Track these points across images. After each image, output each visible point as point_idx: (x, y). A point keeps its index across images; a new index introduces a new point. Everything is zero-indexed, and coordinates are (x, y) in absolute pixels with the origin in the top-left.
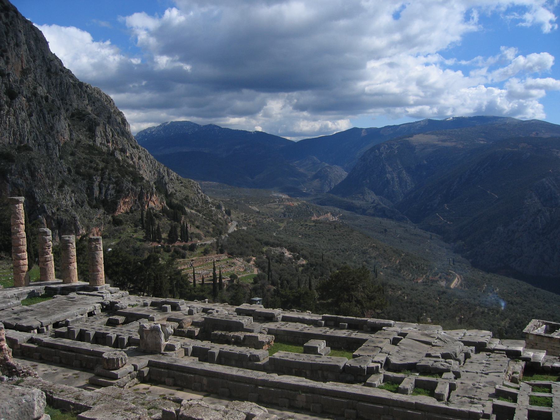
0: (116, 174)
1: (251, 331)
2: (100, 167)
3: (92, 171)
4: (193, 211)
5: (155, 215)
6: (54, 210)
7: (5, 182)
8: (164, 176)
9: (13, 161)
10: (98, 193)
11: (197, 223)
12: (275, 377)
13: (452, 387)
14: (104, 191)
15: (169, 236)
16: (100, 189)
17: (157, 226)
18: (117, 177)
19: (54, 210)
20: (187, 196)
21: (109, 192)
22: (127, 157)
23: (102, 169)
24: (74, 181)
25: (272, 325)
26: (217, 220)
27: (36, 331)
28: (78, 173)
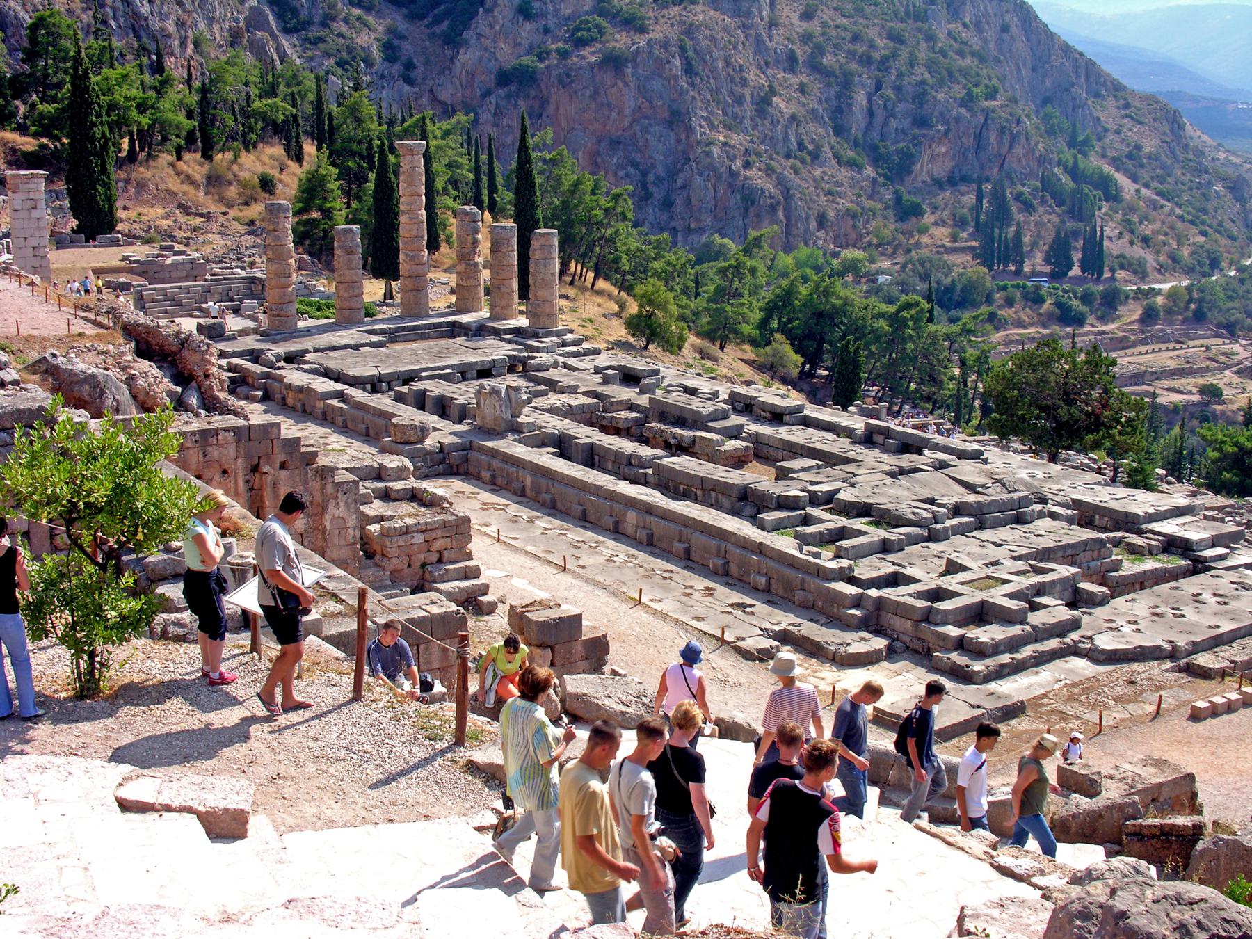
0: (921, 73)
1: (710, 430)
2: (877, 55)
3: (854, 66)
4: (1145, 192)
5: (1018, 197)
6: (737, 165)
7: (620, 84)
8: (1073, 85)
9: (643, 30)
10: (863, 124)
11: (1146, 229)
12: (624, 488)
13: (885, 548)
14: (879, 119)
15: (1047, 261)
16: (871, 113)
17: (1013, 229)
18: (923, 82)
19: (737, 165)
20: (1138, 147)
21: (893, 124)
22: (965, 25)
23: (884, 60)
24: (802, 89)
25: (766, 430)
26: (1221, 225)
27: (368, 387)
28: (815, 67)
